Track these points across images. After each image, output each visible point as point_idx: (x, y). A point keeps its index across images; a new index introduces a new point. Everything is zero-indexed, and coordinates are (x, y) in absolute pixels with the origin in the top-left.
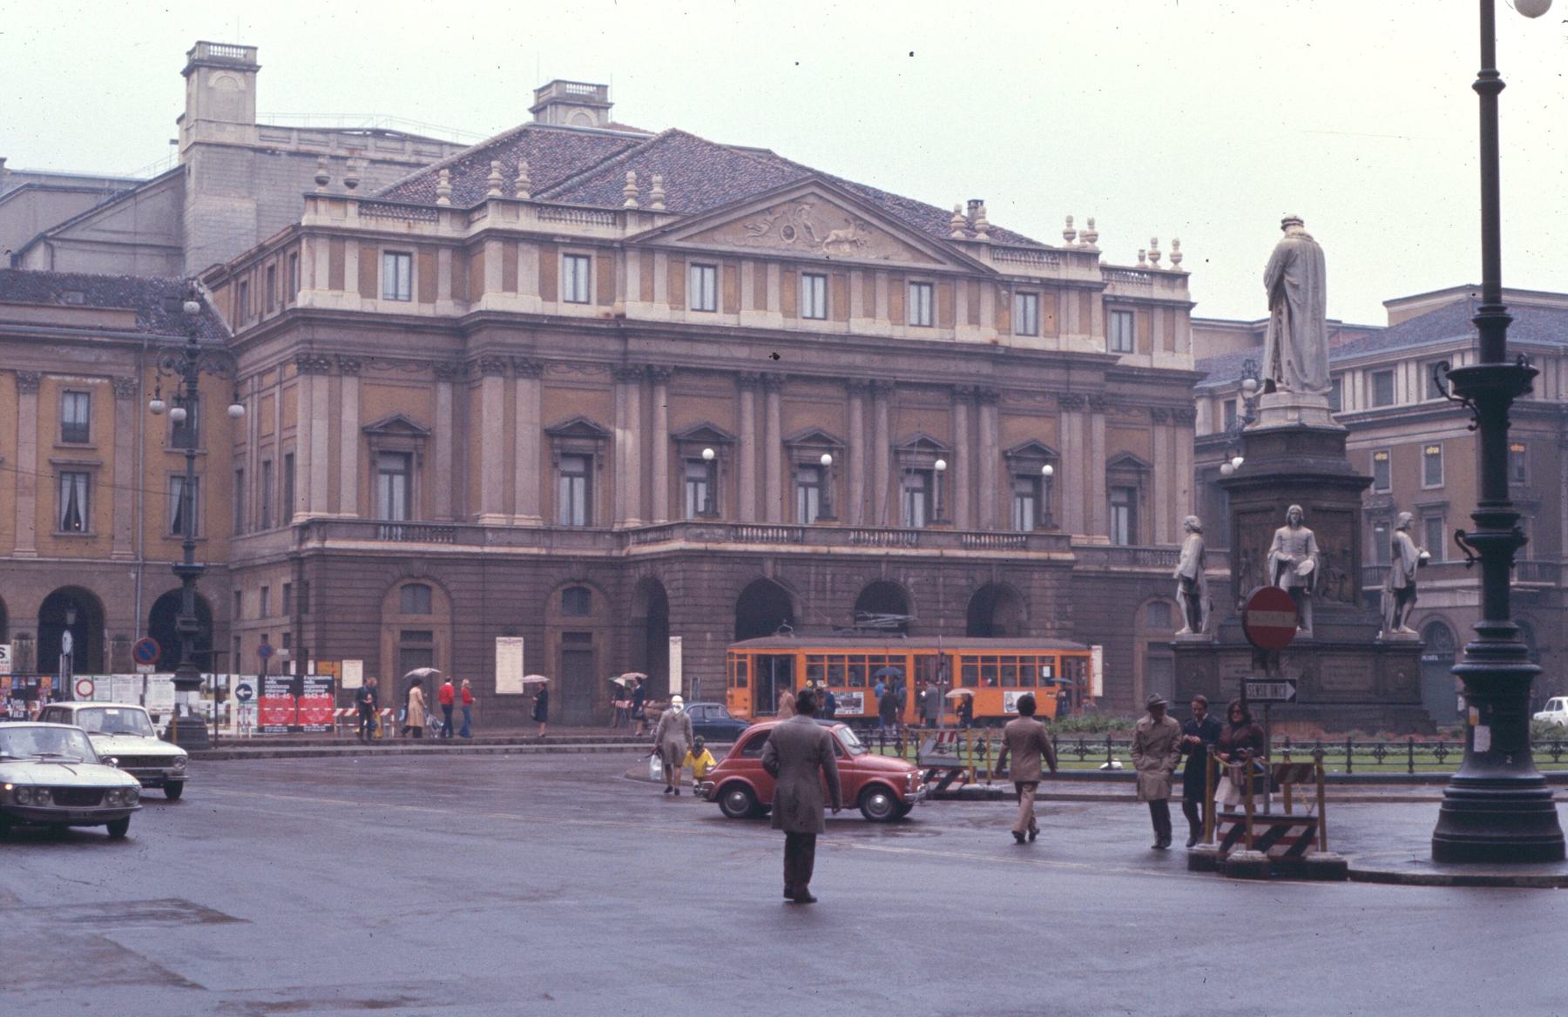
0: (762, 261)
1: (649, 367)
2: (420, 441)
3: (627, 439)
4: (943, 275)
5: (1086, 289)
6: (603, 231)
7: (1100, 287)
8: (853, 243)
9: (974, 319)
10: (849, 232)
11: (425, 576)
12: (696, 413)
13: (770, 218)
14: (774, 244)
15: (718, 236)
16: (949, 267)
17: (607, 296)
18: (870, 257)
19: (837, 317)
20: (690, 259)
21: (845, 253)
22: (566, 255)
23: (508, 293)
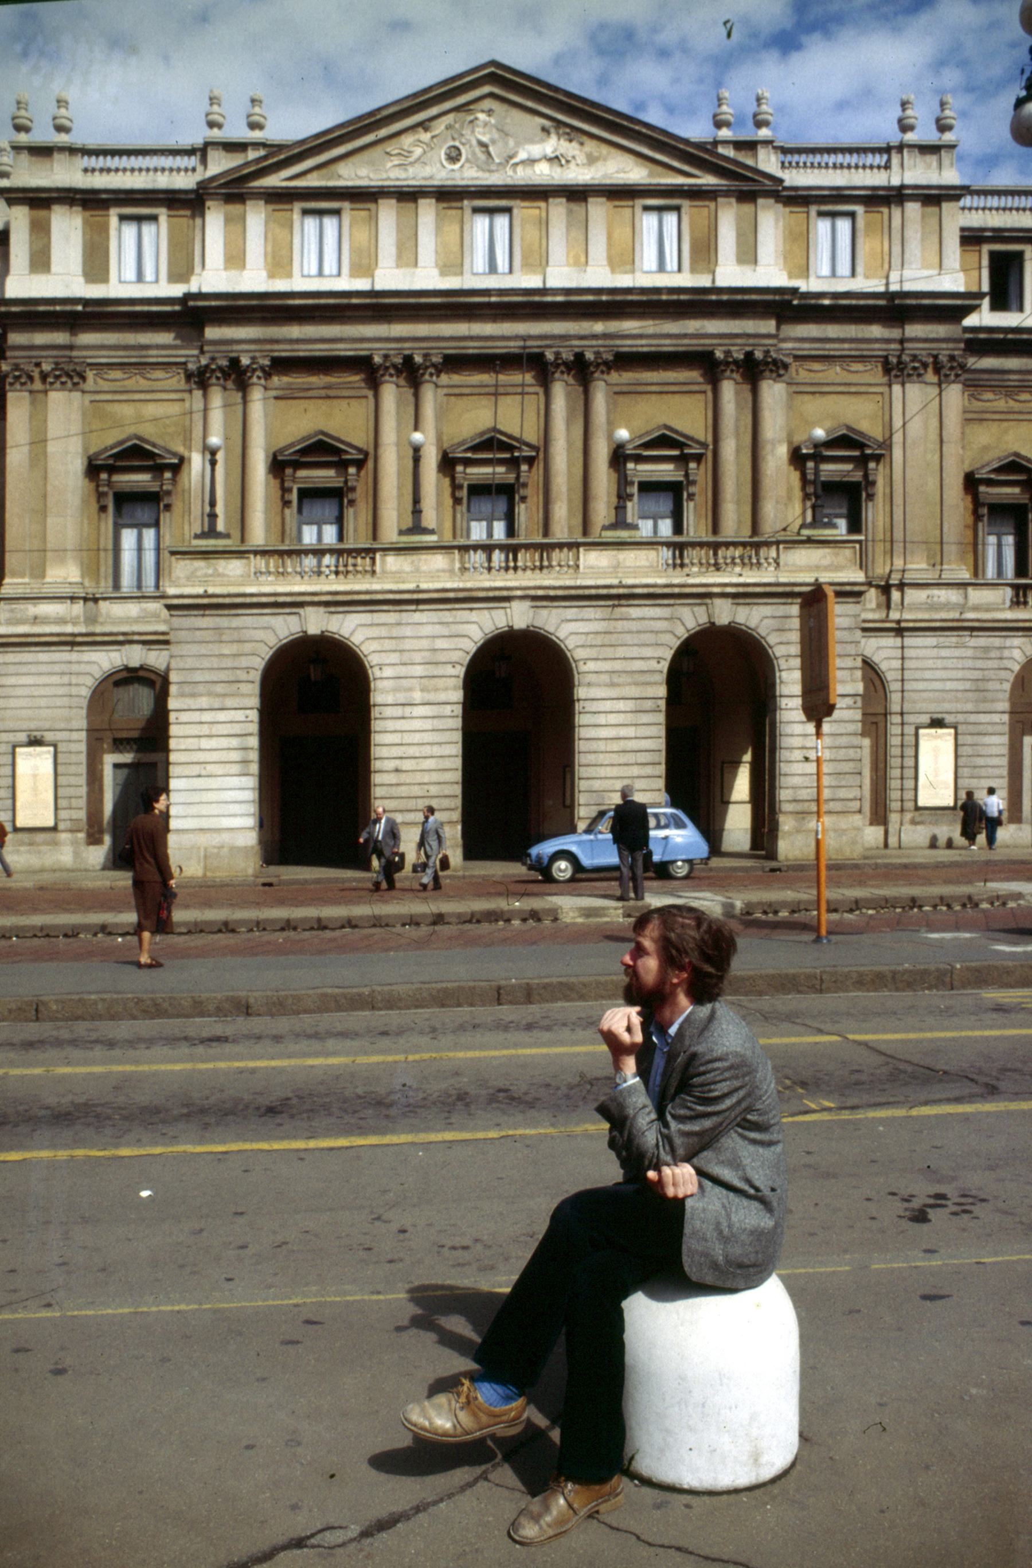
0: (408, 196)
4: (695, 194)
8: (554, 159)
9: (748, 255)
10: (552, 145)
13: (425, 137)
14: (437, 171)
16: (709, 180)
17: (181, 271)
18: (578, 174)
19: (528, 266)
21: (543, 174)
22: (123, 218)
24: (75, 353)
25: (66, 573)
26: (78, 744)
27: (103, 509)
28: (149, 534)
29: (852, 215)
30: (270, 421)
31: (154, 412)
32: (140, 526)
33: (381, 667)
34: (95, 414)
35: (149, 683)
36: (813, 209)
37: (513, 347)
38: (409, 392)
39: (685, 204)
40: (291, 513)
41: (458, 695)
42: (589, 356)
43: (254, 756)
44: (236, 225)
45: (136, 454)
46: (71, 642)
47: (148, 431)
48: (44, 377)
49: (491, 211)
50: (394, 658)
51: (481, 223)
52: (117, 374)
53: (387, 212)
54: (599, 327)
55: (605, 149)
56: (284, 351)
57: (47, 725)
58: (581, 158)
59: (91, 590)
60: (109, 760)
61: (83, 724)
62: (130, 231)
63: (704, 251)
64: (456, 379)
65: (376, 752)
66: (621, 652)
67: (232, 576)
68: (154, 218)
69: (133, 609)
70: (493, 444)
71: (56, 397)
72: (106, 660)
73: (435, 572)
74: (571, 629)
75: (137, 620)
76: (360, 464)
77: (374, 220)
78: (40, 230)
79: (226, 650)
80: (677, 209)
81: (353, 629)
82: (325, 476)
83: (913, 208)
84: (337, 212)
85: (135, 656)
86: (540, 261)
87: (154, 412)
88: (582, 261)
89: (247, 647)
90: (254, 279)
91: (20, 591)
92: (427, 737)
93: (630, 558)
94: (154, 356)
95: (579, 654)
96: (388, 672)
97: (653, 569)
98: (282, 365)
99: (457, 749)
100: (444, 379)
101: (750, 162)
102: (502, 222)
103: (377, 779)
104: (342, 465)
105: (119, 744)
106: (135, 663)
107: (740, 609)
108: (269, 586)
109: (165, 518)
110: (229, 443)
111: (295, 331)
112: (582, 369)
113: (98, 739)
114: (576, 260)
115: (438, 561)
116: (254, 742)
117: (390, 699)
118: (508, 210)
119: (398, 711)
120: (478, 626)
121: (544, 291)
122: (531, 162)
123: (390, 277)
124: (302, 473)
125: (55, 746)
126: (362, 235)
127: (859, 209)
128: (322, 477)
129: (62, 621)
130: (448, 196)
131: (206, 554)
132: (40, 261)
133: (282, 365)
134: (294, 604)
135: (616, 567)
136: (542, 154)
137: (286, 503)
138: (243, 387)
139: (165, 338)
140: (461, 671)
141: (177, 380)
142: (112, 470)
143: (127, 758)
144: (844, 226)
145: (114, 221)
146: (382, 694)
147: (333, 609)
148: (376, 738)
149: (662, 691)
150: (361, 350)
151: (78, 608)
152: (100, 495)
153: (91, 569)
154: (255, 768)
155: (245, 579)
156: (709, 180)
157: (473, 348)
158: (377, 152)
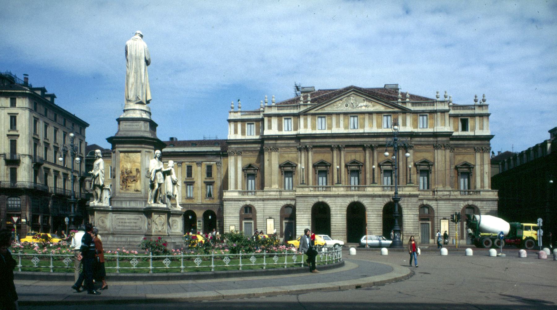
0: (338, 114)
3: (301, 166)
4: (394, 113)
5: (443, 112)
6: (295, 111)
7: (448, 111)
8: (366, 106)
9: (404, 124)
10: (365, 103)
12: (320, 157)
13: (341, 102)
14: (344, 109)
15: (326, 108)
16: (396, 110)
17: (296, 128)
18: (371, 109)
19: (361, 127)
20: (317, 116)
21: (364, 109)
22: (285, 119)
23: (272, 129)
25: (275, 186)
26: (278, 219)
27: (282, 174)
28: (291, 179)
29: (426, 115)
30: (312, 157)
31: (291, 156)
32: (289, 177)
34: (280, 156)
35: (291, 207)
36: (419, 115)
37: (358, 144)
38: (339, 152)
39: (392, 114)
40: (317, 175)
42: (373, 145)
43: (310, 222)
44: (306, 120)
45: (288, 164)
46: (277, 199)
47: (290, 159)
48: (271, 149)
49: (354, 117)
51: (352, 118)
52: (284, 148)
53: (334, 118)
54: (375, 140)
55: (376, 104)
56: (315, 144)
58: (371, 106)
59: (280, 189)
60: (284, 222)
61: (279, 215)
62: (286, 121)
63: (396, 124)
64: (348, 149)
65: (331, 222)
67: (306, 191)
68: (291, 119)
69: (288, 193)
70: (354, 162)
71: (273, 153)
72: (283, 203)
73: (341, 191)
75: (289, 195)
76: (330, 166)
77: (331, 119)
78: (270, 121)
79: (306, 204)
80: (390, 116)
81: (327, 201)
82: (323, 168)
83: (439, 114)
84: (325, 117)
85: (289, 202)
86: (363, 127)
87: (291, 156)
88: (371, 126)
90: (309, 131)
91: (267, 190)
93: (376, 189)
94: (291, 145)
95: (367, 206)
97: (380, 191)
98: (315, 147)
99: (346, 222)
100: (346, 149)
101: (404, 106)
102: (356, 118)
103: (332, 227)
104: (326, 166)
105: (286, 219)
106: (289, 203)
108: (312, 193)
109: (294, 176)
110: (304, 163)
111: (317, 140)
112: (372, 148)
113: (282, 217)
114: (370, 127)
115: (342, 189)
116: (310, 220)
118: (357, 116)
120: (349, 201)
121: (364, 133)
122: (361, 107)
123: (335, 130)
124: (319, 167)
126: (329, 121)
127: (428, 114)
128: (323, 169)
129: (275, 196)
130: (345, 114)
131: (302, 187)
132: (270, 127)
133: (315, 147)
134: (317, 196)
135: (373, 191)
136: (364, 105)
137: (316, 173)
138: (308, 151)
139: (293, 142)
141: (295, 150)
142: (284, 167)
143: (287, 221)
144: (425, 117)
145: (283, 119)
146: (333, 212)
148: (332, 220)
149: (382, 213)
150: (330, 144)
151: (278, 193)
152: (282, 172)
153: (280, 186)
154: (311, 225)
155: (308, 192)
156: (396, 110)
157: (350, 144)
158: (332, 105)
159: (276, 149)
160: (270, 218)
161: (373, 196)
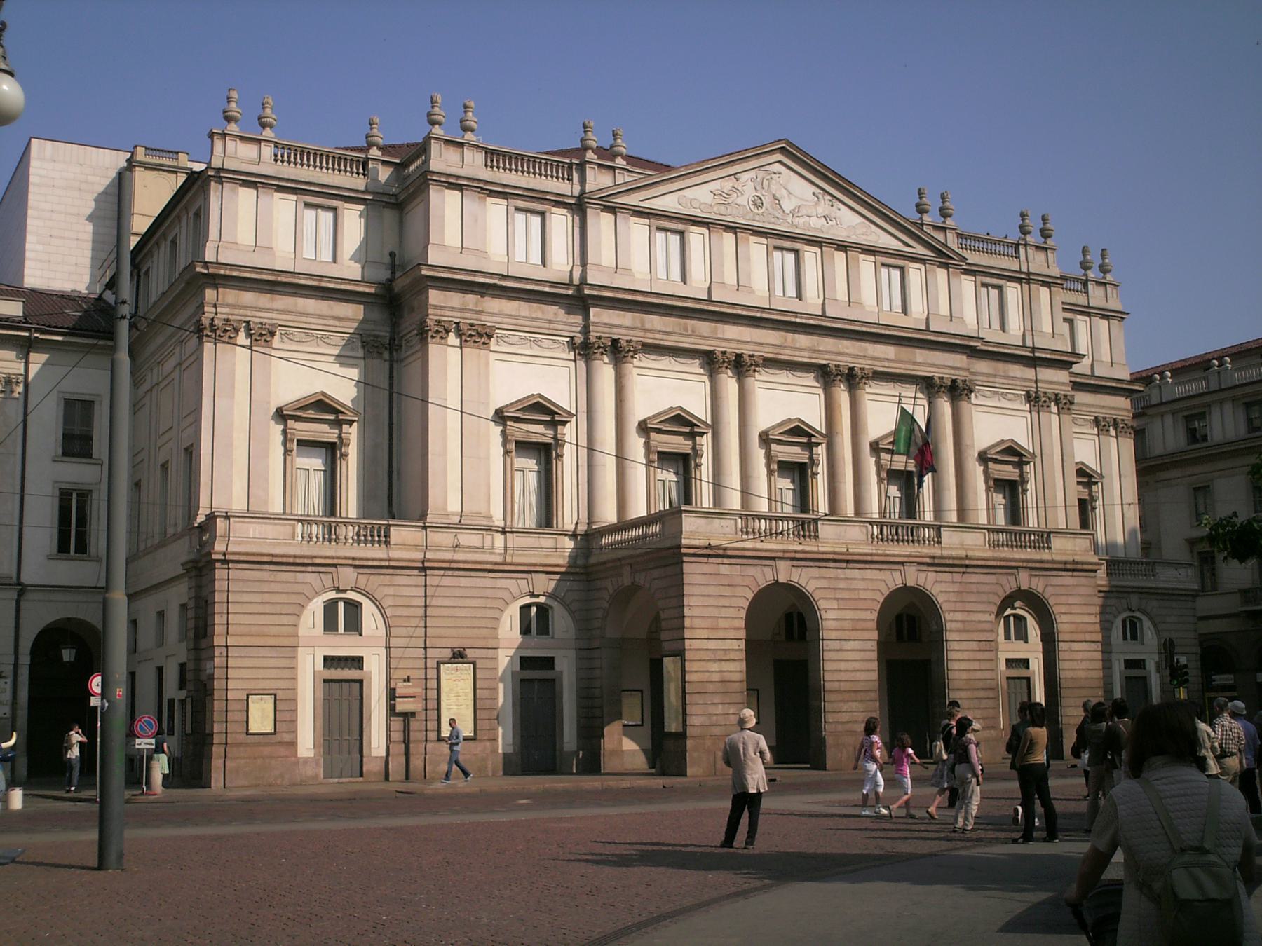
1: (615, 342)
2: (345, 427)
11: (355, 589)
21: (814, 225)
24: (483, 318)
33: (826, 610)
41: (875, 635)
50: (834, 604)
57: (466, 643)
66: (969, 607)
74: (938, 586)
89: (739, 591)
92: (857, 666)
95: (945, 607)
96: (830, 615)
107: (1035, 580)
117: (833, 635)
119: (836, 645)
125: (474, 663)
140: (875, 616)
147: (795, 563)
156: (920, 250)
159: (477, 336)
160: (458, 656)
161: (962, 566)
